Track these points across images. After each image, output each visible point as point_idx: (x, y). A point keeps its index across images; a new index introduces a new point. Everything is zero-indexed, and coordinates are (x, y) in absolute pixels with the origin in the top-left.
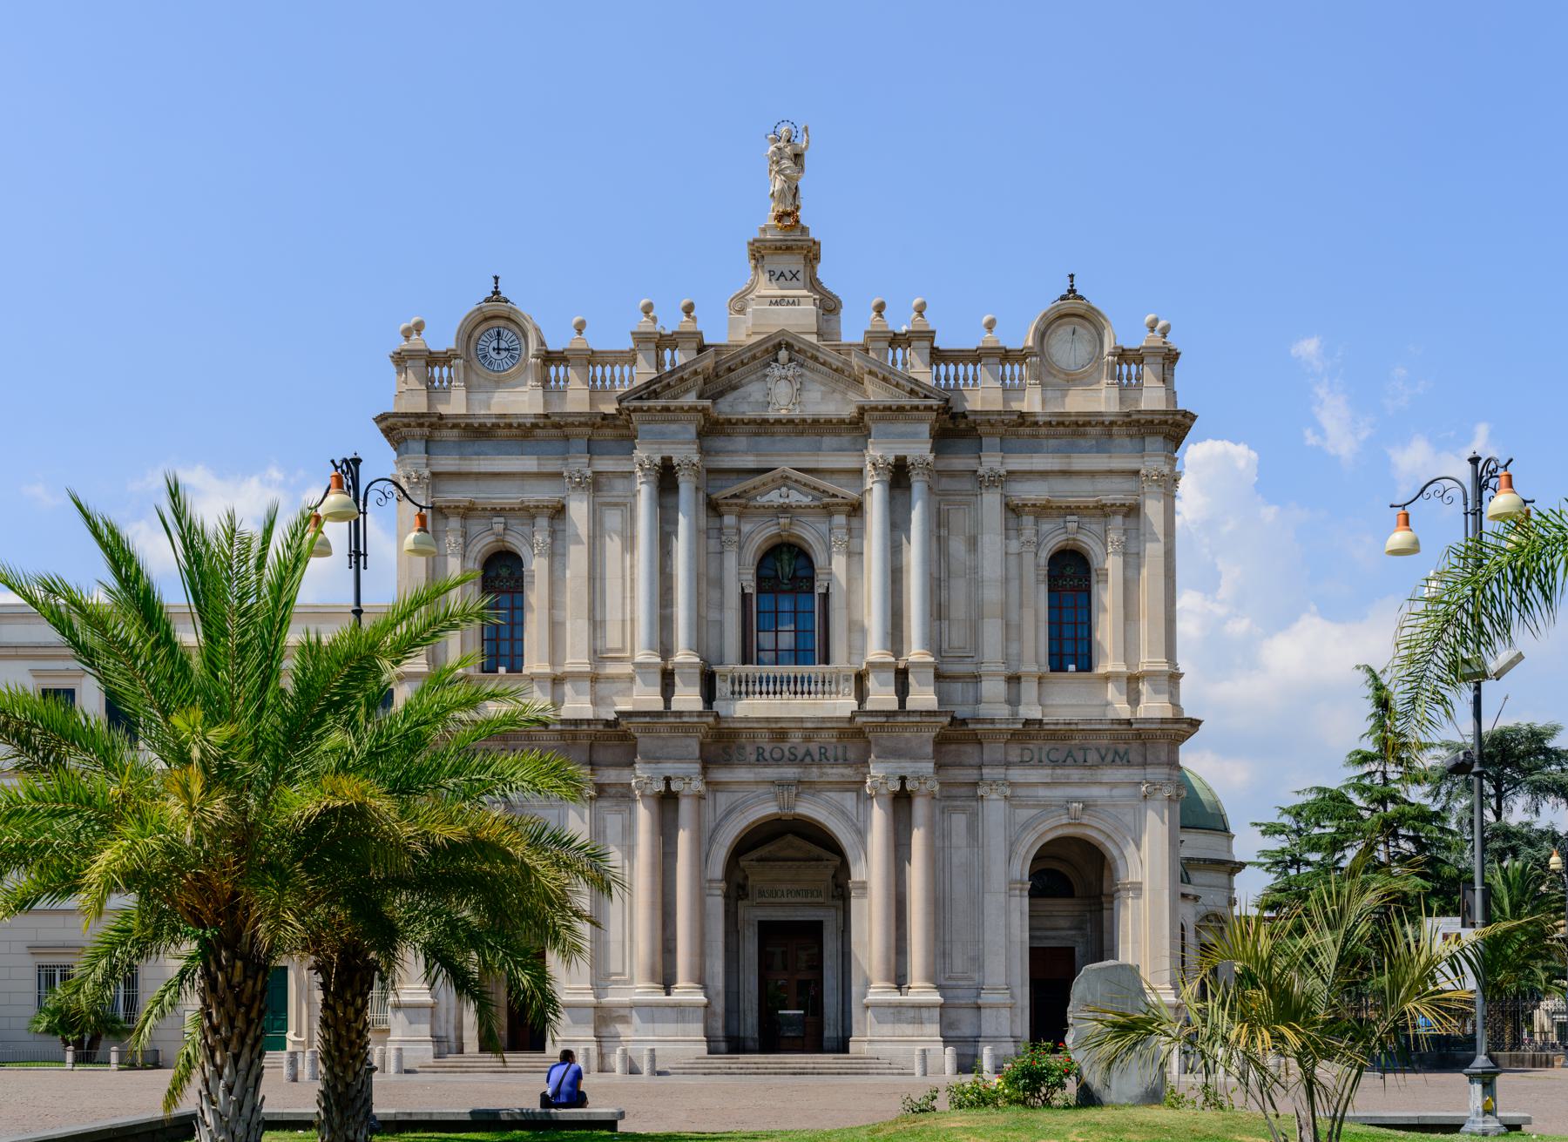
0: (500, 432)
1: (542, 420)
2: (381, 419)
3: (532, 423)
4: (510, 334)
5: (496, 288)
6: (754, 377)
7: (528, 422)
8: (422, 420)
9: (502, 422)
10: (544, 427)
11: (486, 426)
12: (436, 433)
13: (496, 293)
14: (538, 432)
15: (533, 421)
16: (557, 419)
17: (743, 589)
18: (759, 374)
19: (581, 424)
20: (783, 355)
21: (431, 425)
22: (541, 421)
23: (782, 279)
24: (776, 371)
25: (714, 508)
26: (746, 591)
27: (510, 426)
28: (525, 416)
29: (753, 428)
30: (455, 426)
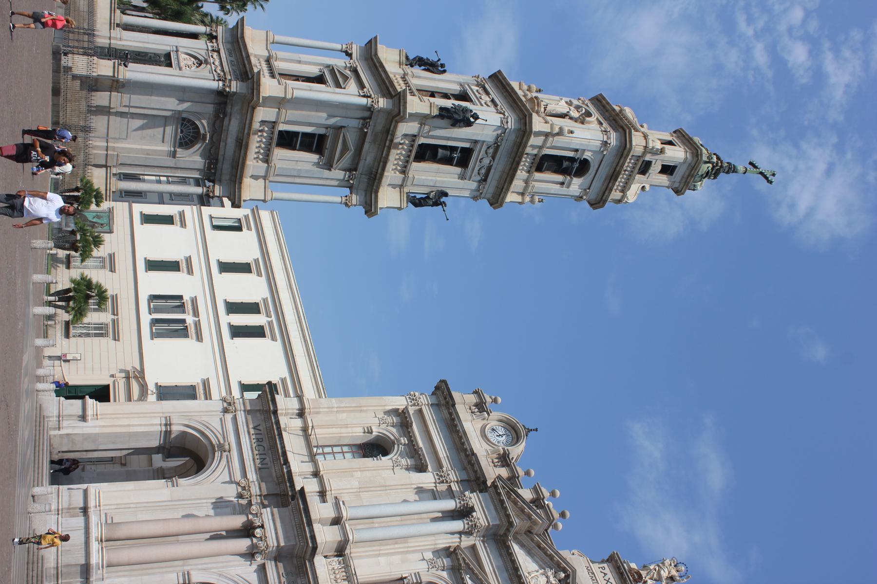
0: (456, 436)
1: (470, 453)
2: (444, 382)
3: (466, 449)
4: (511, 441)
5: (531, 430)
6: (541, 563)
7: (466, 446)
8: (448, 397)
9: (461, 434)
10: (467, 456)
11: (456, 428)
12: (443, 408)
13: (530, 430)
14: (463, 455)
15: (468, 448)
16: (474, 459)
17: (405, 578)
18: (544, 566)
19: (476, 472)
20: (563, 575)
21: (447, 403)
22: (469, 452)
23: (604, 575)
24: (550, 573)
25: (450, 553)
26: (405, 580)
27: (460, 438)
28: (469, 444)
29: (510, 565)
30: (451, 414)
